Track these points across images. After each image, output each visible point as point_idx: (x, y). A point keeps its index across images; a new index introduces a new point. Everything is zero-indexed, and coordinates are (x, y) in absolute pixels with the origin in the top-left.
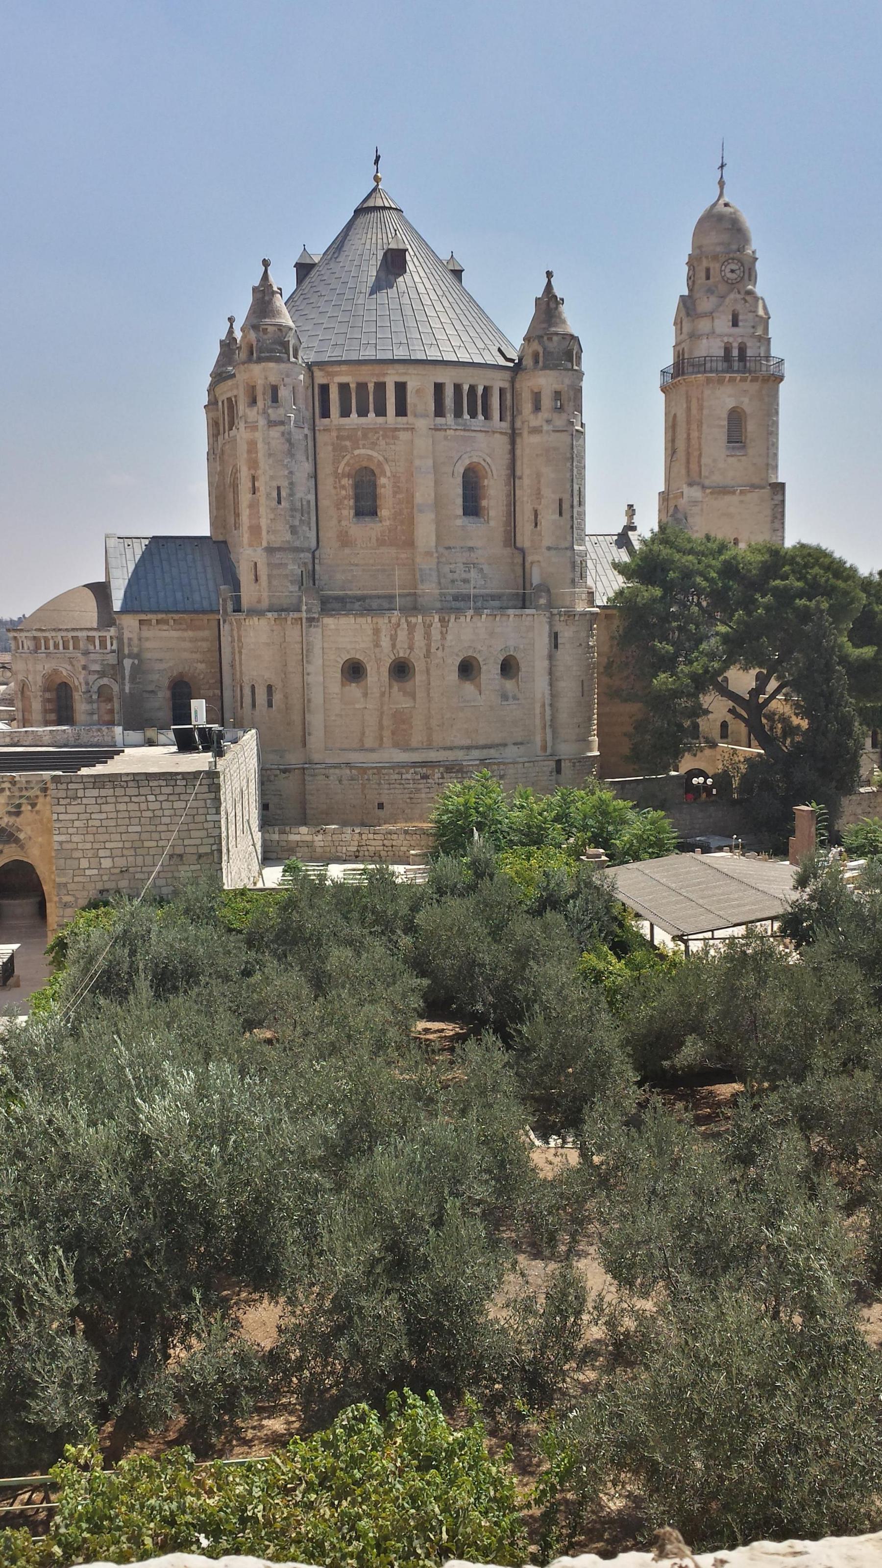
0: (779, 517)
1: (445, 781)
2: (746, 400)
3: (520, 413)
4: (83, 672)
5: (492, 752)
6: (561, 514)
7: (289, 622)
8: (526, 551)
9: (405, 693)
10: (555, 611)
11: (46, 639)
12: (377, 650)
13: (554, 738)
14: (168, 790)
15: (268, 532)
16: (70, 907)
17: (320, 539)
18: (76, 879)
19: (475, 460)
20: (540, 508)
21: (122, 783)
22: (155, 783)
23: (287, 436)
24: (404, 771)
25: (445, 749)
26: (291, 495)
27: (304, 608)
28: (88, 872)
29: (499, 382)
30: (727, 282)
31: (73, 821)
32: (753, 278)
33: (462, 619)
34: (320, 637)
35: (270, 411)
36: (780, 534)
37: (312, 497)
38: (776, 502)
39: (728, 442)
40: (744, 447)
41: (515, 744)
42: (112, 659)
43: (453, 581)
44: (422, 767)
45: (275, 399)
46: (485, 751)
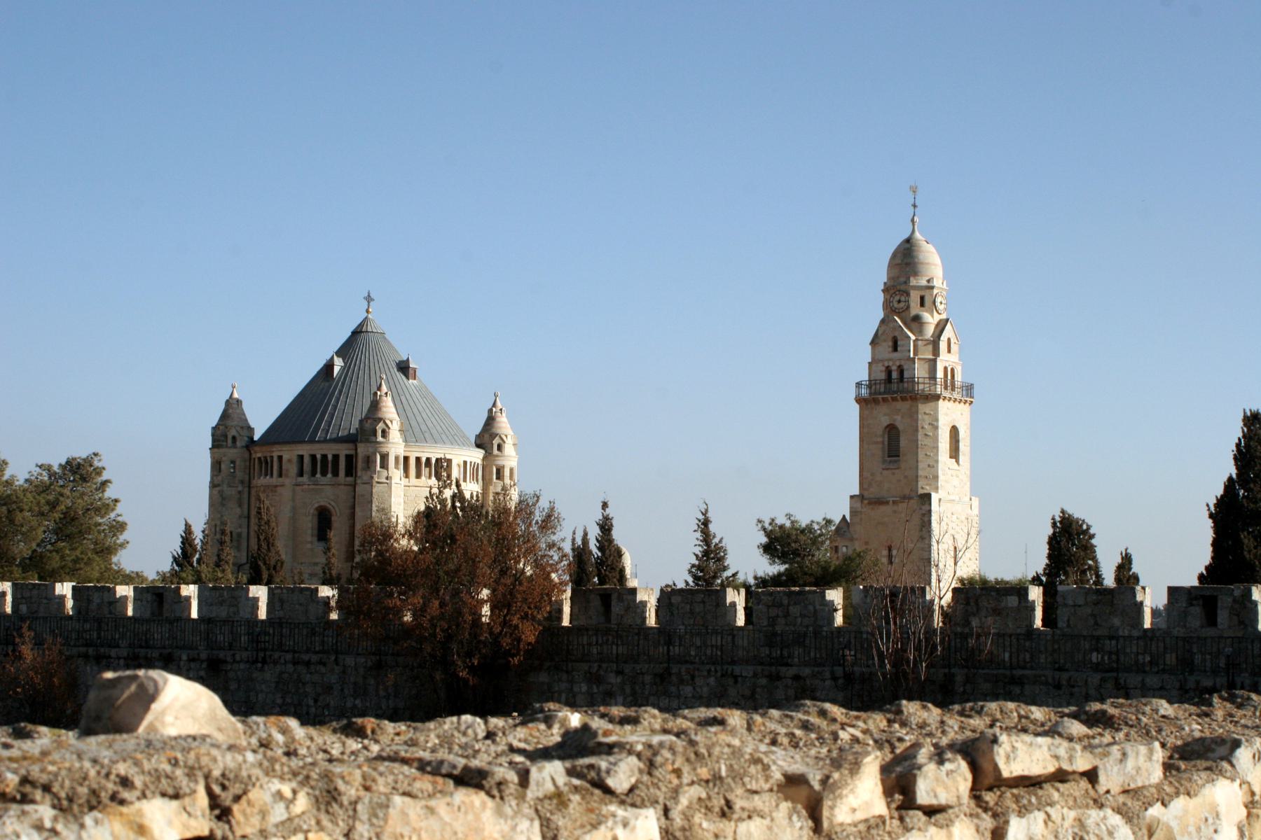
19: (322, 504)
29: (343, 450)
36: (927, 542)
37: (245, 531)
38: (924, 512)
39: (889, 456)
40: (899, 461)
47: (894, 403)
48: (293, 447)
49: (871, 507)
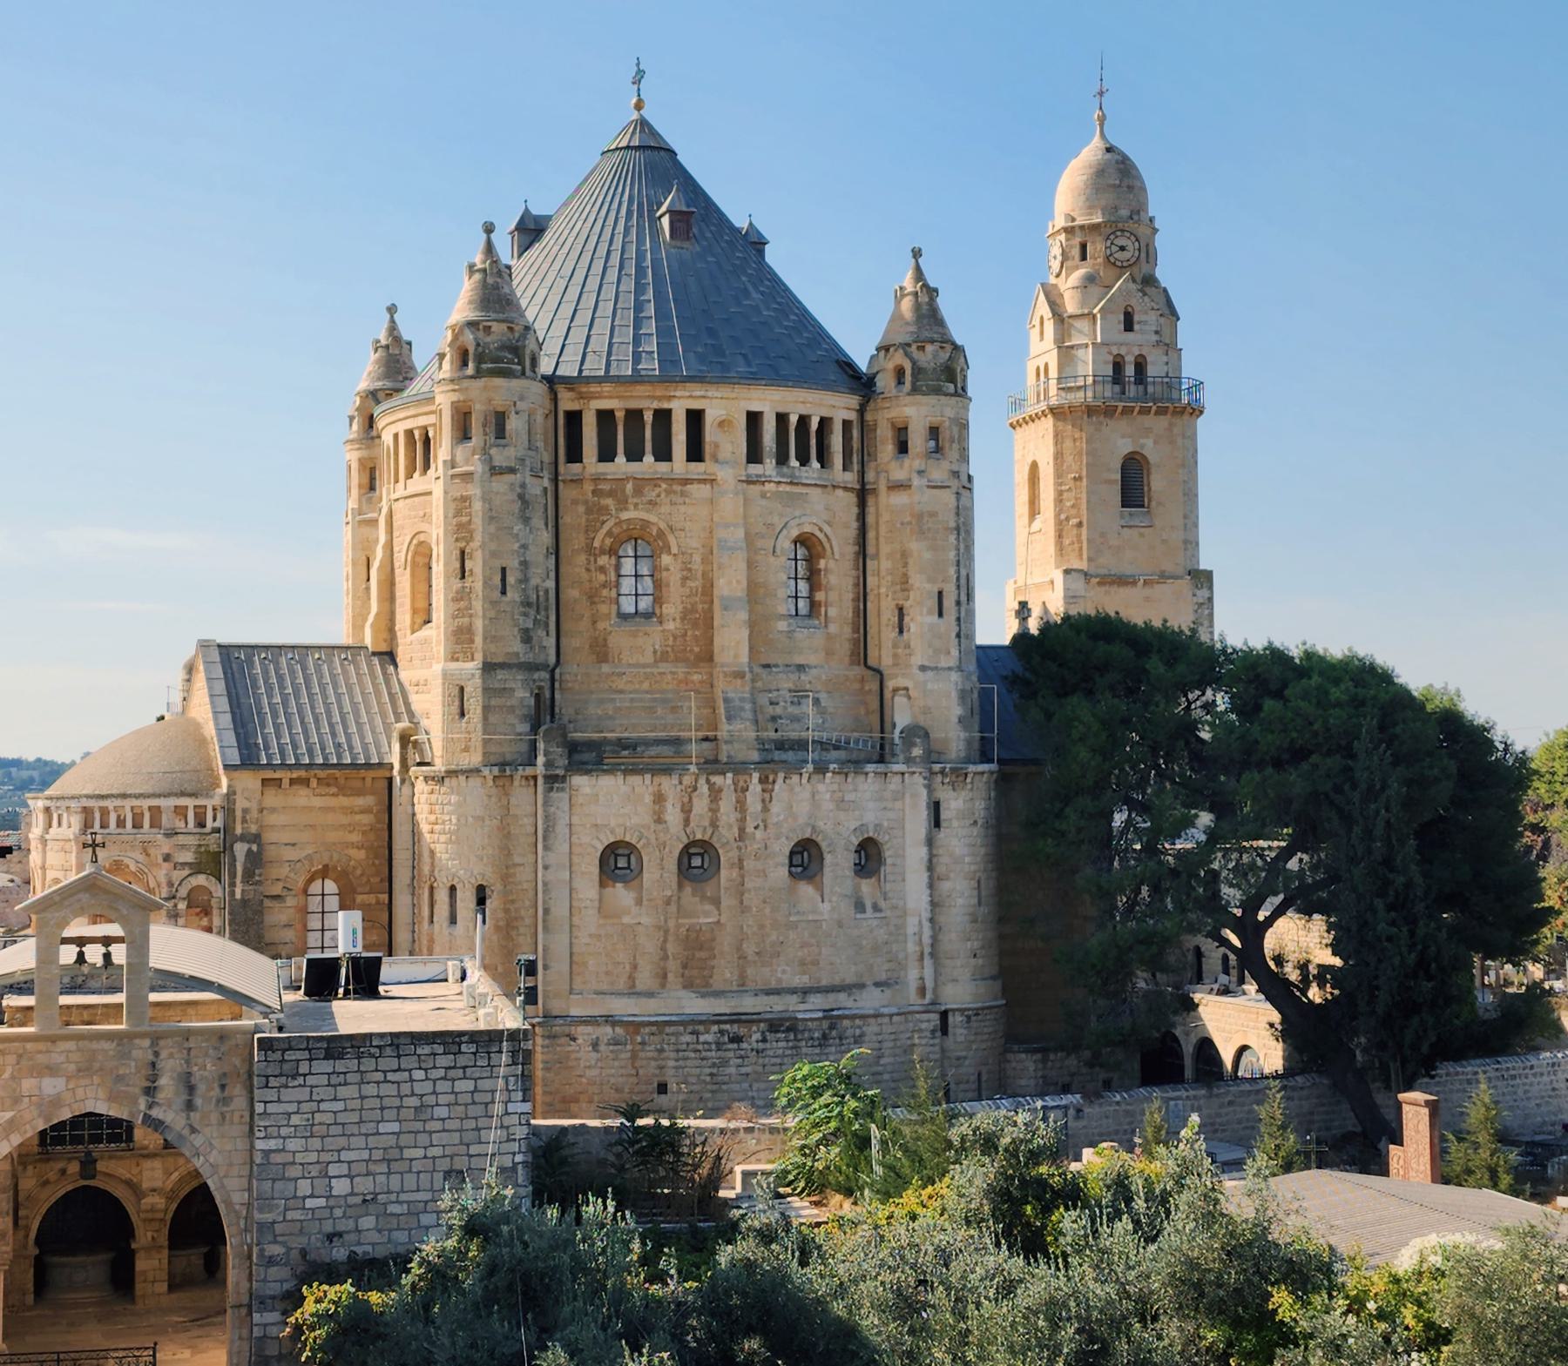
0: (1206, 623)
1: (768, 1045)
2: (1149, 442)
3: (873, 456)
4: (166, 864)
5: (842, 996)
6: (940, 614)
7: (516, 783)
8: (885, 673)
9: (703, 898)
10: (937, 767)
11: (104, 812)
12: (660, 827)
13: (937, 974)
14: (444, 1061)
15: (485, 639)
16: (277, 1264)
17: (562, 651)
18: (290, 1215)
19: (807, 529)
20: (907, 604)
21: (373, 1050)
22: (426, 1050)
23: (519, 490)
24: (701, 1028)
25: (769, 992)
26: (525, 580)
27: (541, 760)
28: (309, 1203)
30: (1114, 264)
31: (289, 1114)
32: (1151, 260)
33: (795, 778)
34: (566, 808)
35: (493, 451)
37: (551, 584)
38: (1201, 601)
41: (877, 984)
42: (214, 842)
43: (774, 719)
44: (732, 1022)
45: (500, 432)
46: (832, 997)
47: (1141, 418)
48: (740, 391)
49: (1103, 589)
